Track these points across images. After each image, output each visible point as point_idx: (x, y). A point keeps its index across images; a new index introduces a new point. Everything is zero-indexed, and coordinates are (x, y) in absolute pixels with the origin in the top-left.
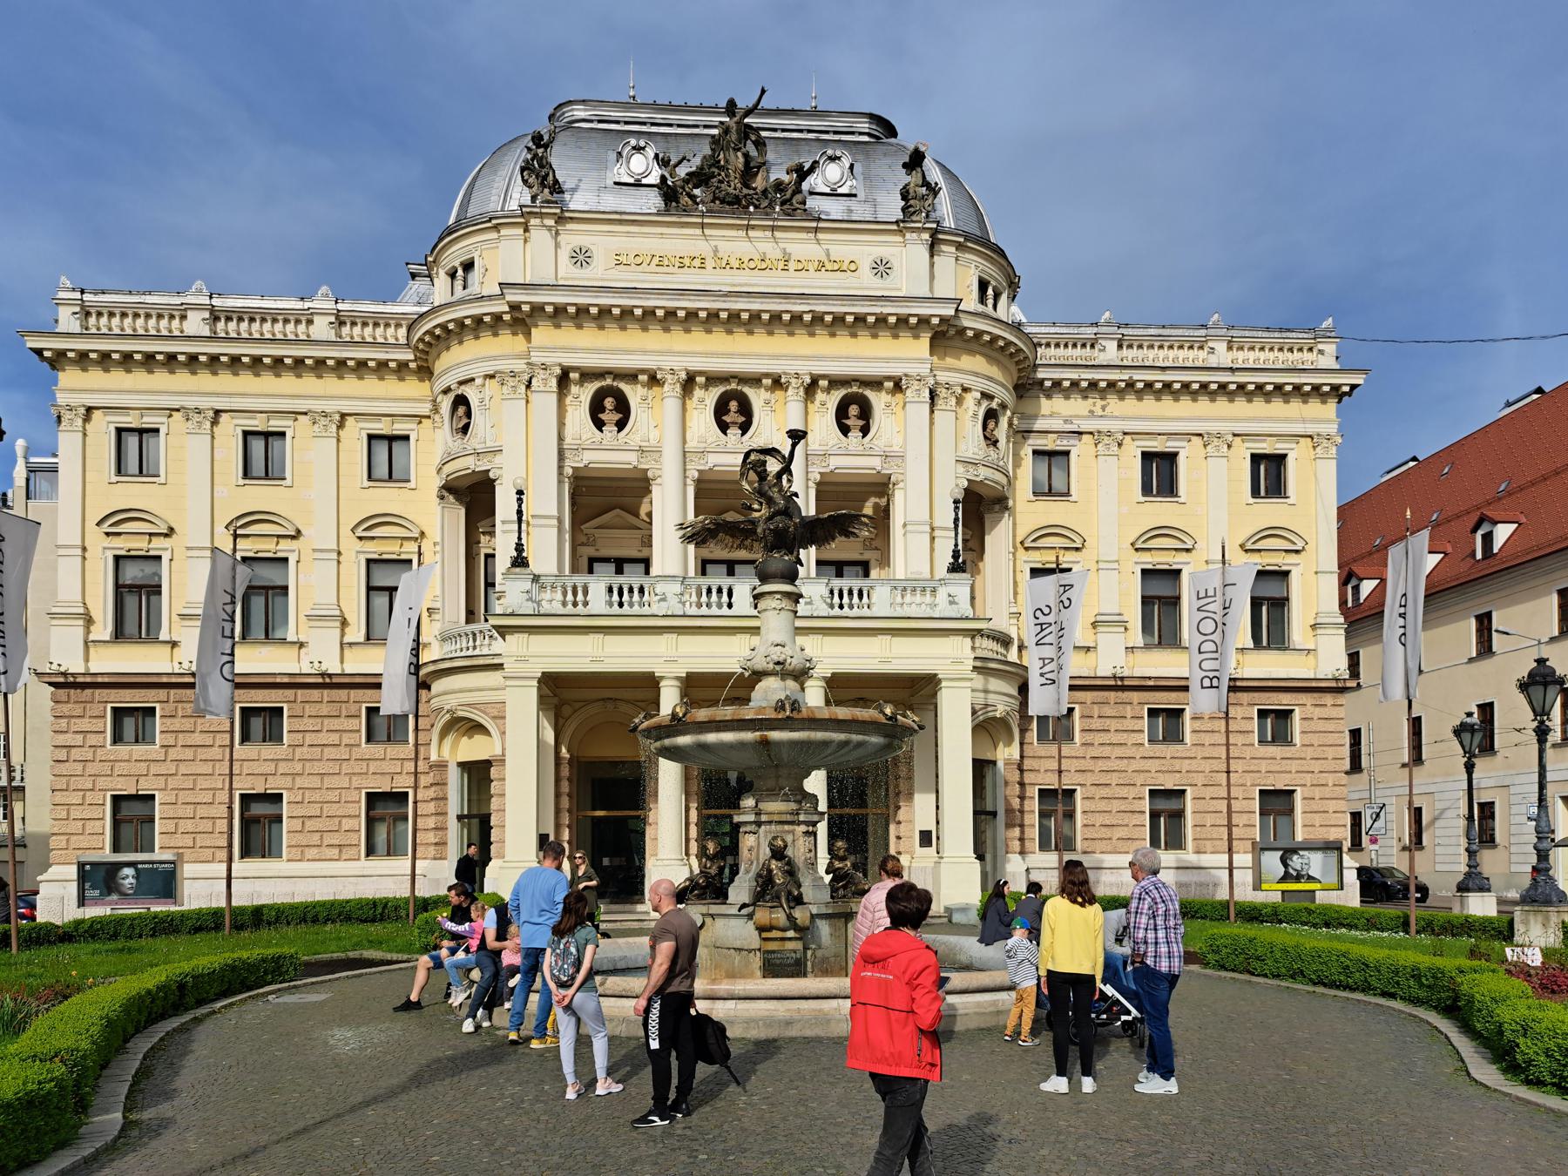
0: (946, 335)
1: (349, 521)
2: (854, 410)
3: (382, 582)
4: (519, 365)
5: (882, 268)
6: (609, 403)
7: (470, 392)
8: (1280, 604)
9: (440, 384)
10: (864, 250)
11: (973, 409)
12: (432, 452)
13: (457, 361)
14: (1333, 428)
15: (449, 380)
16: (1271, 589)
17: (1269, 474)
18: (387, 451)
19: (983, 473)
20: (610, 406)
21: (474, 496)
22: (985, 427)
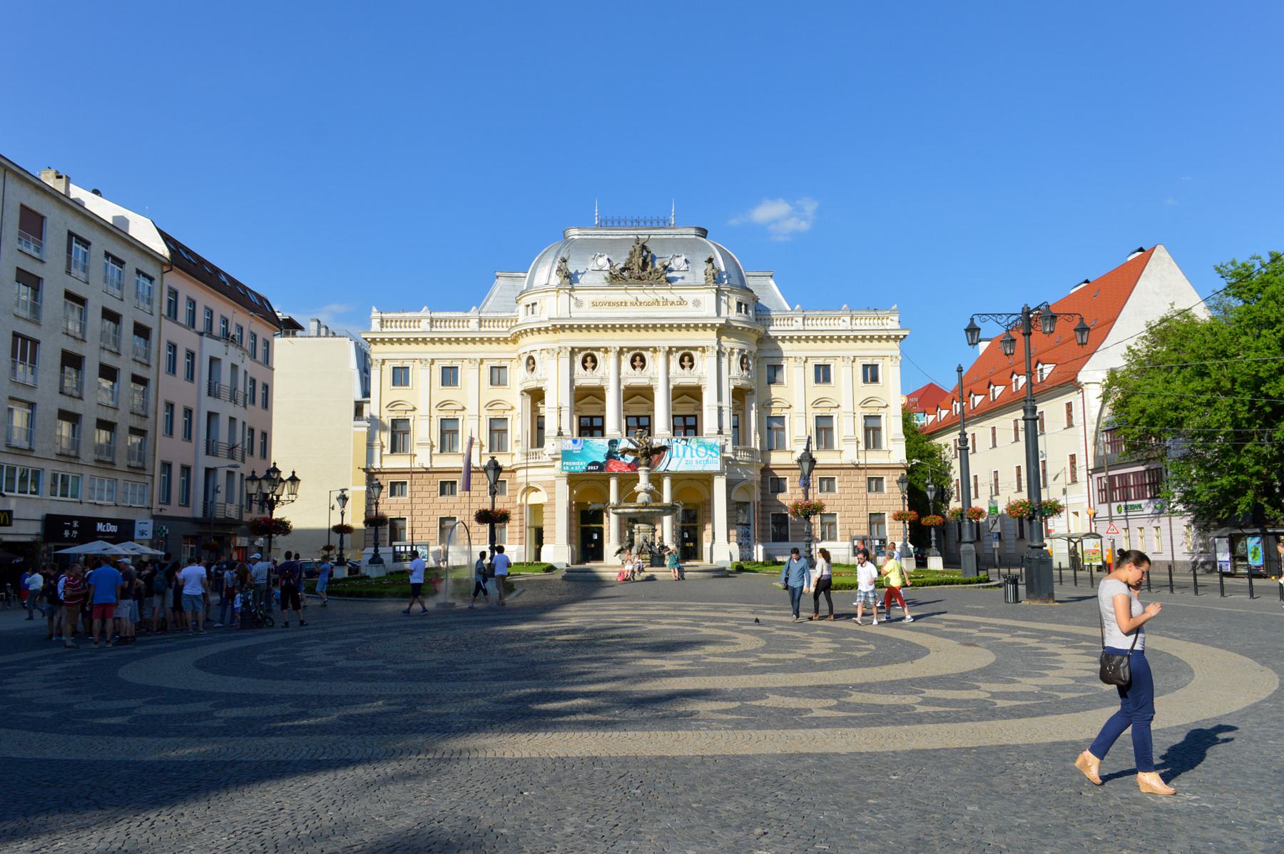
0: (725, 330)
1: (483, 403)
2: (686, 358)
3: (497, 430)
4: (555, 346)
5: (697, 303)
6: (589, 359)
7: (533, 354)
8: (877, 430)
9: (521, 351)
10: (689, 296)
11: (735, 359)
12: (518, 378)
13: (529, 344)
14: (898, 353)
15: (528, 349)
16: (871, 423)
17: (871, 373)
18: (497, 375)
19: (739, 383)
20: (590, 360)
21: (537, 395)
22: (742, 362)
